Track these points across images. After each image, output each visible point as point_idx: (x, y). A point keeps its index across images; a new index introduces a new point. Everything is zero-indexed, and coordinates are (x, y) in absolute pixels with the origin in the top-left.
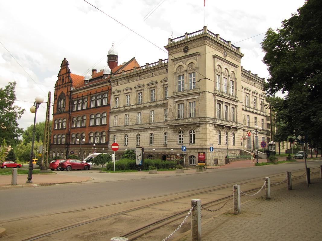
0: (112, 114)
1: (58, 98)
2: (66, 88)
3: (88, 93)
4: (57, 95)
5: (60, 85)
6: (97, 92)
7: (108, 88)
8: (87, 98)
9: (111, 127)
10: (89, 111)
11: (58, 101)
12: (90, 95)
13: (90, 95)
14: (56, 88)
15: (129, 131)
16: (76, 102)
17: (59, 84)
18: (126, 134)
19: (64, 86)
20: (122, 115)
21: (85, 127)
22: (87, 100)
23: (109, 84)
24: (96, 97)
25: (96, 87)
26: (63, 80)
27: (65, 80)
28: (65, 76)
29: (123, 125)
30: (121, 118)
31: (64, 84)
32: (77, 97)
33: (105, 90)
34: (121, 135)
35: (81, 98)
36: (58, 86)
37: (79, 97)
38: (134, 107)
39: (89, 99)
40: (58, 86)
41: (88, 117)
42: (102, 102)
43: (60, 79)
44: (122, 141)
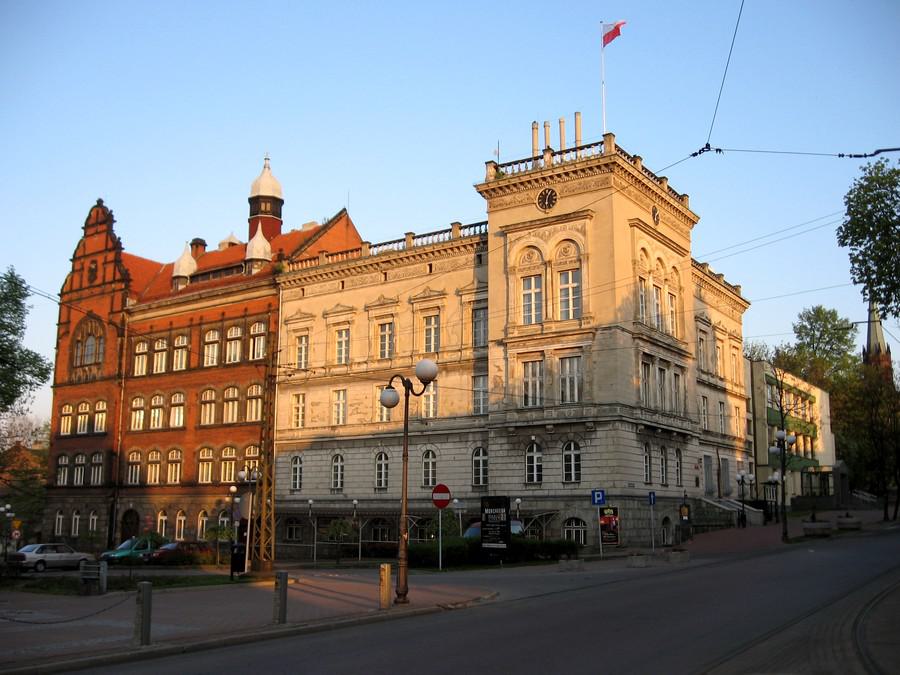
0: (286, 389)
1: (71, 332)
2: (107, 300)
3: (192, 320)
4: (68, 322)
5: (81, 289)
6: (227, 316)
7: (270, 305)
8: (189, 336)
9: (280, 431)
10: (195, 377)
11: (75, 343)
12: (200, 324)
13: (200, 324)
14: (66, 298)
15: (350, 445)
16: (142, 348)
17: (76, 285)
18: (337, 451)
19: (97, 290)
20: (320, 392)
21: (183, 429)
22: (190, 342)
23: (274, 291)
24: (223, 332)
25: (224, 300)
26: (93, 273)
27: (100, 274)
28: (100, 259)
29: (326, 424)
30: (317, 404)
31: (99, 286)
32: (148, 330)
33: (256, 311)
34: (319, 458)
35: (164, 334)
36: (71, 291)
37: (155, 329)
38: (364, 367)
39: (195, 338)
40: (71, 291)
41: (194, 398)
42: (245, 350)
43: (83, 269)
44: (323, 475)
